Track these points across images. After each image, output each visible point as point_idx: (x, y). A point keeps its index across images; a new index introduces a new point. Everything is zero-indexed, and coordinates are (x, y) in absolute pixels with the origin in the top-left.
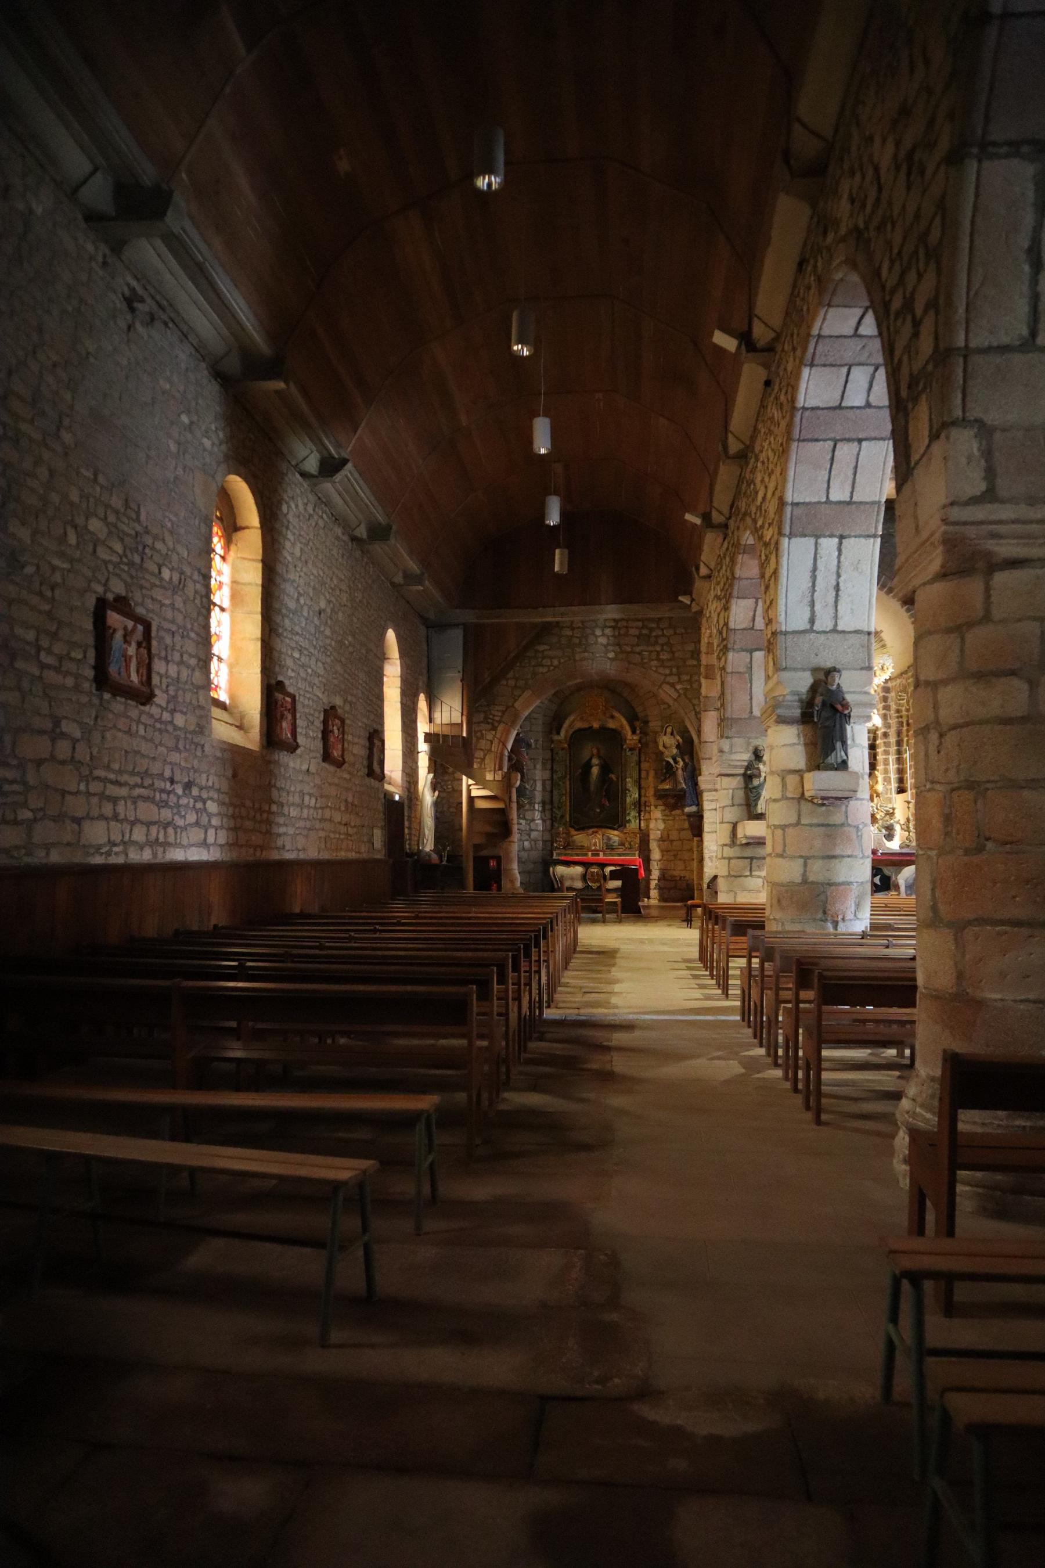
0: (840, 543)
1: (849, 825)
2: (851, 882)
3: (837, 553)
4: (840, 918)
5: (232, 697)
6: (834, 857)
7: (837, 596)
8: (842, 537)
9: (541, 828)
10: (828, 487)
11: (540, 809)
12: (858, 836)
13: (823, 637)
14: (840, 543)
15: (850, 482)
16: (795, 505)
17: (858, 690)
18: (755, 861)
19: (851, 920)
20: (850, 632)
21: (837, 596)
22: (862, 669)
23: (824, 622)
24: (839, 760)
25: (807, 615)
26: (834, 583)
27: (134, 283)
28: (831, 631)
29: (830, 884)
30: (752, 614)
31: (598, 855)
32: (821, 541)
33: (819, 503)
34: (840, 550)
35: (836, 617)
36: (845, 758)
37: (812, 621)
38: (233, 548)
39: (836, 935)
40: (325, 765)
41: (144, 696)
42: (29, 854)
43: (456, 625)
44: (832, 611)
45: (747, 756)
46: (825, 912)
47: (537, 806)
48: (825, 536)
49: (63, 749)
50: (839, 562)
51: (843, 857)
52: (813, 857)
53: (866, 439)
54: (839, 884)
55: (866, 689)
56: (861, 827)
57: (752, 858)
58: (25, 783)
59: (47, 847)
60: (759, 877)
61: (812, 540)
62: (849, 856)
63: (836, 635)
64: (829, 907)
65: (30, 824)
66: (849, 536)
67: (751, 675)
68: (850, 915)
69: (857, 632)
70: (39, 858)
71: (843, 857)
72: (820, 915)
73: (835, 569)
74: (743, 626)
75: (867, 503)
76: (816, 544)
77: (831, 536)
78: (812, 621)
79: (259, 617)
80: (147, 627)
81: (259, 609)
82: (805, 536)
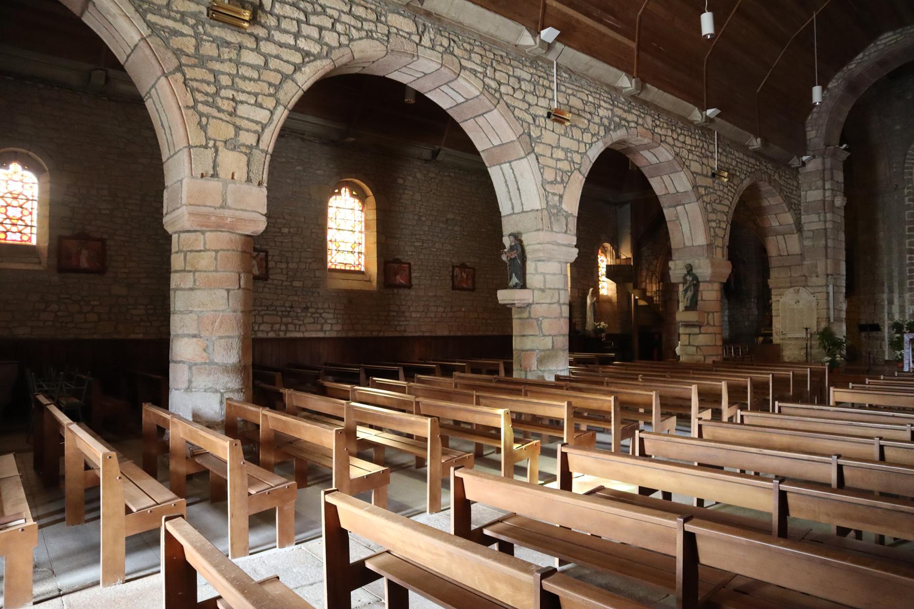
0: (511, 165)
1: (531, 318)
3: (511, 171)
4: (528, 369)
5: (366, 268)
6: (524, 336)
7: (520, 192)
8: (510, 162)
9: (756, 313)
11: (756, 301)
12: (538, 325)
13: (518, 216)
15: (495, 134)
16: (483, 151)
18: (691, 336)
19: (534, 371)
20: (529, 211)
21: (520, 192)
22: (536, 230)
23: (518, 209)
24: (514, 283)
25: (510, 206)
32: (502, 166)
34: (512, 168)
37: (513, 209)
38: (365, 206)
40: (454, 291)
43: (627, 202)
44: (519, 202)
47: (753, 300)
50: (514, 175)
51: (529, 336)
53: (484, 113)
54: (527, 351)
56: (540, 319)
57: (689, 334)
61: (498, 167)
62: (532, 335)
63: (524, 214)
64: (522, 363)
66: (513, 161)
69: (532, 210)
72: (519, 367)
73: (514, 180)
76: (501, 169)
77: (505, 163)
78: (513, 209)
79: (376, 233)
80: (267, 252)
81: (376, 230)
82: (494, 165)
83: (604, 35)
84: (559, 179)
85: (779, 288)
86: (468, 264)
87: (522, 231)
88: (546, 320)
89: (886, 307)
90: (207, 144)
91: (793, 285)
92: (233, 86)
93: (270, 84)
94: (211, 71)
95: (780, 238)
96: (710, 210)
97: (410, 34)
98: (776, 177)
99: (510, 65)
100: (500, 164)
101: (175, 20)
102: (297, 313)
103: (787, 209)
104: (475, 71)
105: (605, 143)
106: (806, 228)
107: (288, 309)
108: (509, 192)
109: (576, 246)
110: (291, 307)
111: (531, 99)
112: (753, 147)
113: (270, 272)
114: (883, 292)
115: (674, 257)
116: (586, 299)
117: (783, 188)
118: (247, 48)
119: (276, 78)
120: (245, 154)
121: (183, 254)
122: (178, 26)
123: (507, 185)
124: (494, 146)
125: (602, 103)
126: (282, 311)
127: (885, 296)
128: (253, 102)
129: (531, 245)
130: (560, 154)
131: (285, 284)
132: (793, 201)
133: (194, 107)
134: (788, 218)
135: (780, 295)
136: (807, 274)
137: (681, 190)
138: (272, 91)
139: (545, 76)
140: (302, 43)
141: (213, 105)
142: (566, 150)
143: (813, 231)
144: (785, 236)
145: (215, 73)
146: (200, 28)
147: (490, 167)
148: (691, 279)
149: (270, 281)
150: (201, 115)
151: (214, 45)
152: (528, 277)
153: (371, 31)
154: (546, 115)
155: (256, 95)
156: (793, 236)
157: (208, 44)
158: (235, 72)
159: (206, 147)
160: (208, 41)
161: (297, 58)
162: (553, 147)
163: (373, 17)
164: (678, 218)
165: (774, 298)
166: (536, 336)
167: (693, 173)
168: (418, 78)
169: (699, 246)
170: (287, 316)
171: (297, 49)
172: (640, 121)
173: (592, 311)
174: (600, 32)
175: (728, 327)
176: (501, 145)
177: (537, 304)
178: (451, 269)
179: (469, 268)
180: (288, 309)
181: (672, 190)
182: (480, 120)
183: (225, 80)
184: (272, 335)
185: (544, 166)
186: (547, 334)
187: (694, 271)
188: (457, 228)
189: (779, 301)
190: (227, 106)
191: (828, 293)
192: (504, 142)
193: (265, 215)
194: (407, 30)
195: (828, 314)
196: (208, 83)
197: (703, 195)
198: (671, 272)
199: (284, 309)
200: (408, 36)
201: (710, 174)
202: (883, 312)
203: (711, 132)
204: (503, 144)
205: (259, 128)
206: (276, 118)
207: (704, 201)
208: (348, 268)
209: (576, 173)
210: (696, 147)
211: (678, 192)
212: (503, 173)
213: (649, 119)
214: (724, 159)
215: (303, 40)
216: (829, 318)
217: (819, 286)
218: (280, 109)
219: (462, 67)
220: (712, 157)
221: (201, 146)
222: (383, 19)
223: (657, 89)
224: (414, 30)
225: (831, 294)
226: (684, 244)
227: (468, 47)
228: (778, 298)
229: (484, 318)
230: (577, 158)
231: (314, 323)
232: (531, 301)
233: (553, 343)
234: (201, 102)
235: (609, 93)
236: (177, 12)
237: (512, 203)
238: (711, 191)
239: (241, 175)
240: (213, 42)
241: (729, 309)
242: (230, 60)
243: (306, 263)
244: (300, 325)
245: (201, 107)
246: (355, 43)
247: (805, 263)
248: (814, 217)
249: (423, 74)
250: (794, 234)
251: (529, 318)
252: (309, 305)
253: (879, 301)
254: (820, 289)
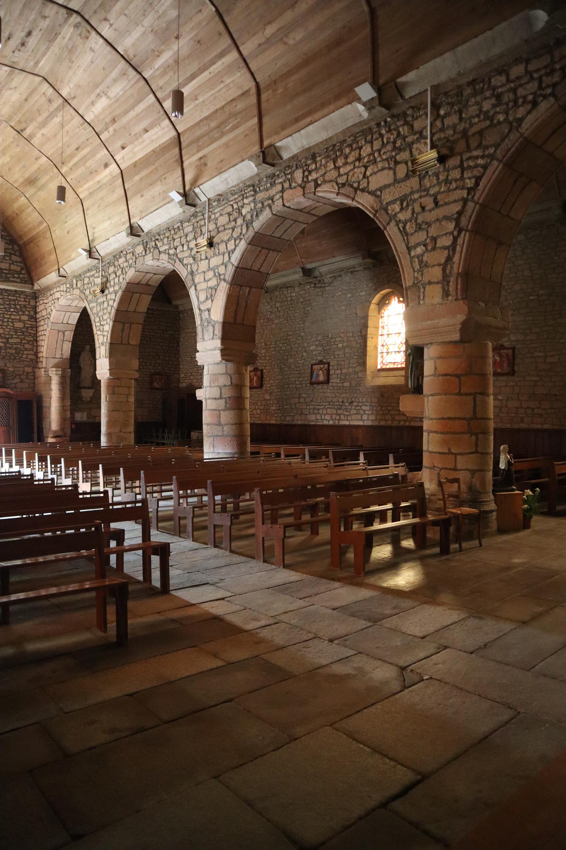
27: (331, 275)
41: (327, 381)
42: (293, 421)
49: (302, 400)
58: (292, 408)
59: (298, 420)
65: (293, 416)
70: (295, 422)
80: (329, 364)
102: (346, 406)
107: (341, 404)
110: (343, 402)
113: (331, 378)
126: (337, 406)
131: (339, 385)
149: (330, 384)
170: (340, 409)
179: (508, 349)
180: (341, 404)
184: (331, 423)
199: (338, 404)
208: (395, 366)
231: (357, 414)
243: (352, 367)
244: (347, 415)
252: (353, 399)
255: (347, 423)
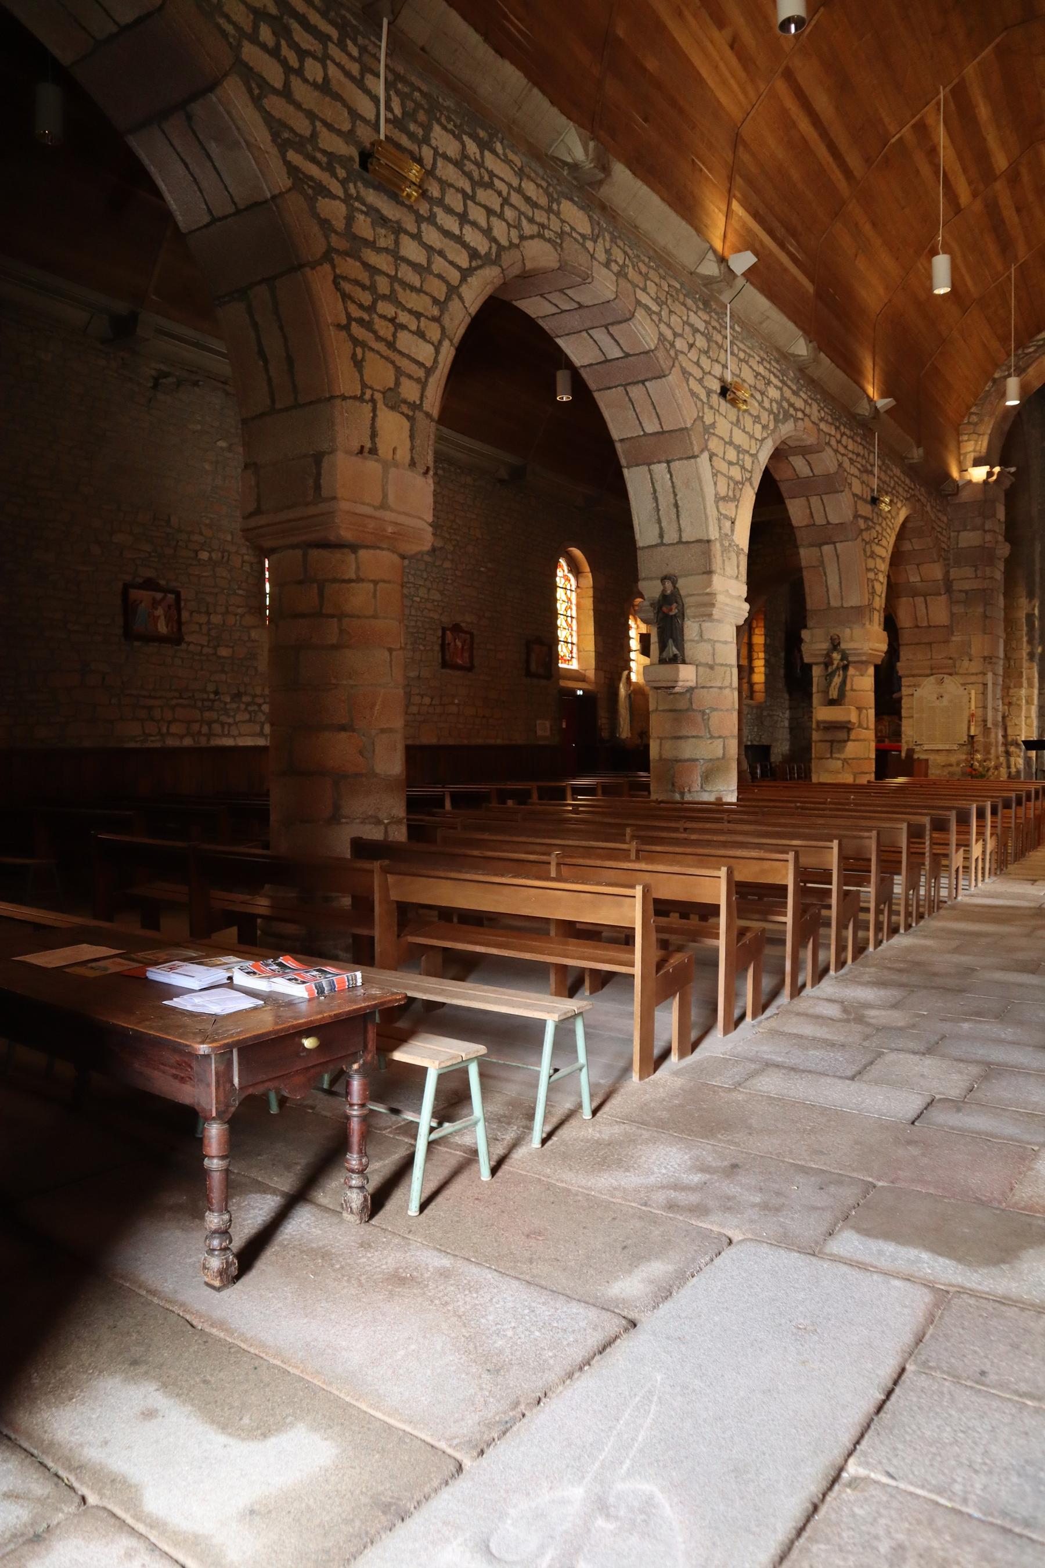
0: (669, 467)
1: (694, 710)
2: (697, 760)
7: (678, 511)
8: (668, 462)
10: (640, 423)
13: (671, 549)
14: (669, 467)
15: (654, 414)
16: (622, 440)
17: (700, 592)
18: (835, 744)
21: (678, 511)
22: (704, 573)
23: (671, 536)
24: (671, 655)
25: (657, 532)
26: (673, 501)
28: (677, 543)
29: (677, 761)
30: (808, 511)
31: (884, 741)
32: (652, 467)
33: (639, 436)
34: (670, 472)
35: (680, 530)
36: (676, 651)
37: (661, 536)
39: (682, 803)
40: (443, 671)
41: (176, 639)
44: (676, 526)
45: (826, 645)
46: (673, 785)
48: (654, 463)
50: (672, 483)
51: (688, 737)
52: (666, 738)
53: (646, 380)
55: (708, 590)
57: (832, 742)
60: (839, 759)
61: (646, 468)
62: (693, 737)
63: (681, 546)
66: (674, 460)
67: (824, 569)
68: (696, 787)
71: (688, 737)
74: (805, 523)
75: (676, 430)
76: (650, 470)
77: (659, 462)
78: (661, 536)
80: (178, 595)
82: (637, 465)
83: (786, 270)
84: (731, 494)
85: (913, 676)
86: (463, 625)
87: (677, 572)
88: (715, 713)
89: (1024, 708)
90: (363, 394)
91: (934, 671)
92: (392, 298)
93: (435, 301)
94: (366, 265)
95: (920, 600)
96: (868, 554)
97: (583, 236)
98: (928, 508)
99: (684, 304)
100: (649, 464)
101: (318, 163)
102: (226, 703)
103: (935, 557)
104: (650, 309)
105: (774, 442)
106: (956, 586)
107: (212, 696)
108: (658, 510)
109: (746, 600)
110: (216, 693)
111: (705, 362)
112: (911, 461)
113: (184, 629)
114: (1021, 686)
115: (810, 624)
116: (617, 688)
117: (935, 526)
118: (406, 232)
119: (439, 290)
120: (407, 417)
121: (315, 585)
122: (324, 177)
123: (656, 499)
124: (646, 434)
125: (772, 378)
126: (203, 700)
127: (1023, 692)
128: (414, 328)
129: (693, 595)
130: (732, 455)
131: (206, 650)
132: (944, 546)
133: (347, 328)
134: (936, 571)
135: (914, 686)
136: (954, 656)
137: (834, 519)
138: (436, 312)
139: (718, 327)
140: (471, 236)
141: (368, 326)
142: (739, 449)
143: (966, 592)
144: (928, 598)
145: (373, 270)
146: (351, 185)
147: (628, 467)
148: (839, 657)
149: (184, 646)
150: (356, 342)
151: (369, 220)
152: (687, 646)
153: (542, 226)
154: (719, 391)
155: (418, 315)
156: (939, 598)
157: (362, 217)
158: (393, 273)
159: (361, 399)
160: (362, 212)
161: (463, 261)
162: (726, 443)
163: (543, 201)
164: (822, 562)
165: (905, 691)
166: (701, 737)
167: (855, 495)
168: (563, 311)
169: (852, 607)
170: (211, 709)
171: (459, 240)
172: (807, 411)
173: (628, 705)
174: (781, 264)
175: (788, 737)
176: (658, 433)
177: (703, 687)
178: (440, 633)
179: (466, 632)
180: (212, 696)
181: (820, 520)
182: (635, 392)
183: (383, 285)
184: (188, 742)
185: (718, 471)
186: (716, 735)
187: (843, 646)
188: (447, 565)
189: (912, 695)
190: (384, 329)
191: (985, 685)
192: (665, 429)
193: (431, 525)
194: (582, 231)
195: (985, 715)
196: (364, 287)
197: (862, 530)
198: (804, 647)
199: (205, 696)
200: (581, 241)
201: (869, 498)
202: (1019, 716)
203: (871, 432)
204: (663, 432)
205: (421, 373)
206: (441, 358)
207: (863, 540)
209: (747, 484)
210: (858, 455)
211: (828, 523)
212: (652, 478)
213: (815, 406)
214: (883, 475)
215: (470, 229)
216: (985, 721)
217: (973, 674)
218: (446, 343)
219: (638, 302)
220: (871, 473)
221: (355, 398)
222: (555, 206)
223: (829, 361)
224: (589, 232)
225: (990, 685)
226: (829, 603)
227: (644, 269)
228: (909, 691)
229: (484, 717)
230: (748, 461)
231: (250, 721)
232: (693, 684)
233: (724, 748)
234: (355, 320)
235: (777, 362)
236: (324, 152)
237: (661, 528)
238: (870, 524)
239: (403, 455)
240: (366, 214)
241: (790, 708)
242: (386, 250)
243: (236, 615)
244: (230, 725)
245: (356, 330)
246: (525, 243)
247: (954, 639)
248: (968, 572)
249: (576, 306)
250: (941, 595)
251: (690, 709)
252: (242, 689)
253: (1015, 699)
254: (973, 679)
255: (229, 742)
